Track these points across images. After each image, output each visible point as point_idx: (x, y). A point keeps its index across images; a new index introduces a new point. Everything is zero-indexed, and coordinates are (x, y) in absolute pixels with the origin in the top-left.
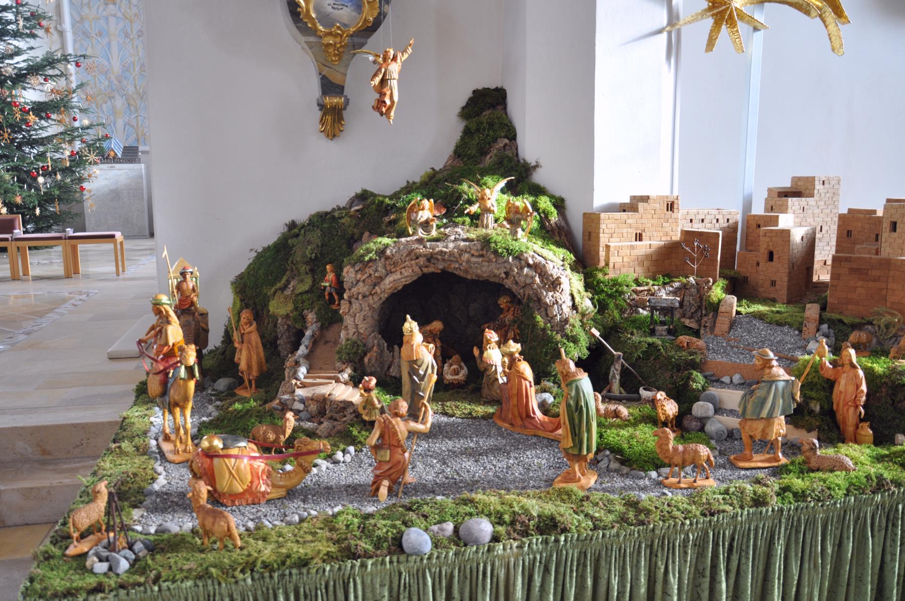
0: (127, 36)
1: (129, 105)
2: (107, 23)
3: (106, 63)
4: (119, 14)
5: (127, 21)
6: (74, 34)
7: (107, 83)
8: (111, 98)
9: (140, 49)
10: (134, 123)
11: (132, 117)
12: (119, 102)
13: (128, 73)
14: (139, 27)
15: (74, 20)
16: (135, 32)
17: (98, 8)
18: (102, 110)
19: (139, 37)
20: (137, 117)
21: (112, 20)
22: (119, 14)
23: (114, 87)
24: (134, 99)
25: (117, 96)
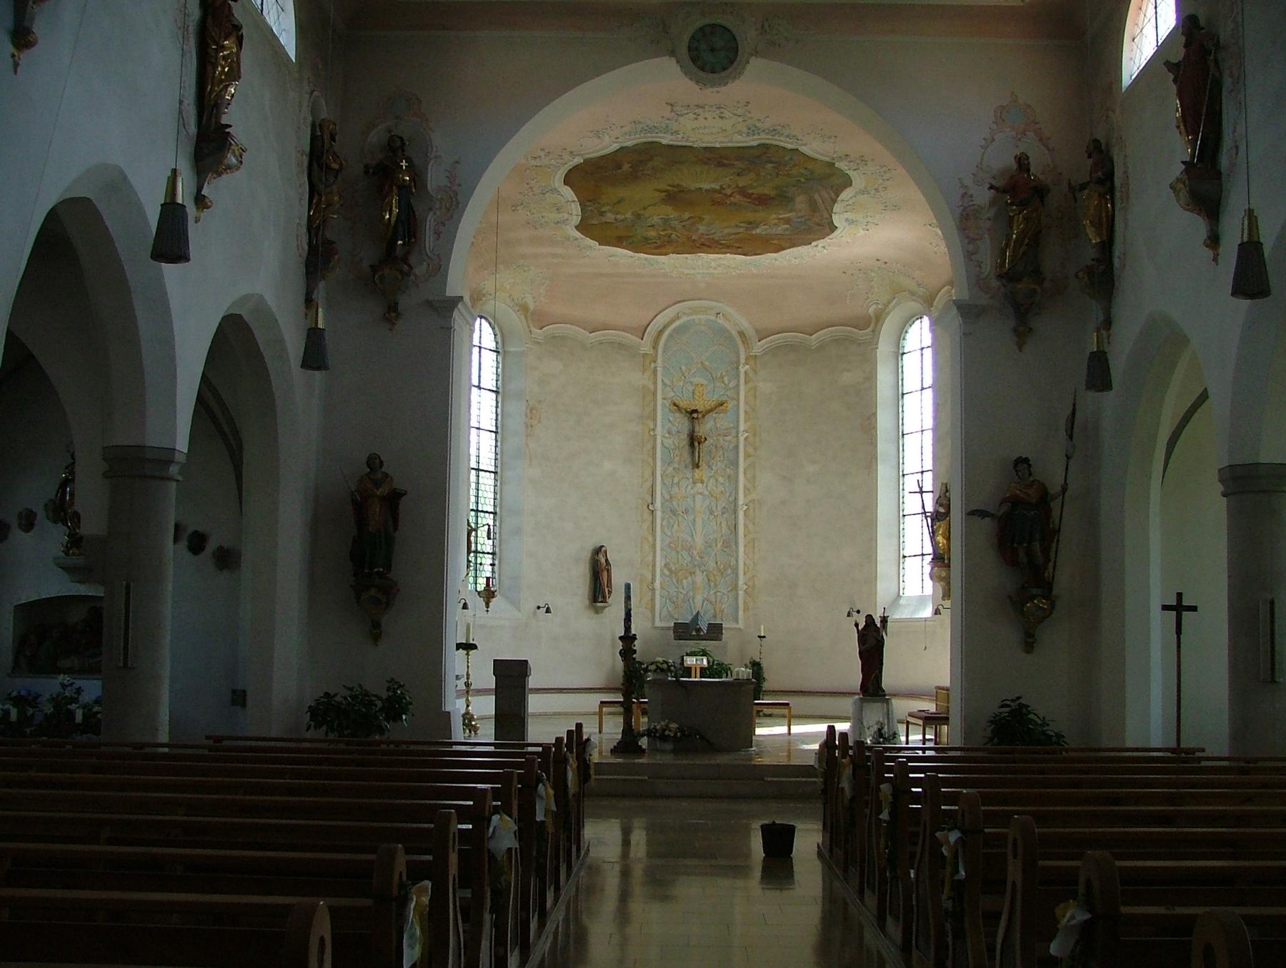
2: (694, 501)
3: (690, 539)
5: (713, 499)
6: (663, 512)
8: (693, 573)
9: (724, 525)
11: (712, 592)
12: (700, 578)
14: (724, 505)
18: (682, 583)
19: (723, 513)
20: (716, 592)
21: (699, 498)
23: (696, 563)
25: (698, 572)
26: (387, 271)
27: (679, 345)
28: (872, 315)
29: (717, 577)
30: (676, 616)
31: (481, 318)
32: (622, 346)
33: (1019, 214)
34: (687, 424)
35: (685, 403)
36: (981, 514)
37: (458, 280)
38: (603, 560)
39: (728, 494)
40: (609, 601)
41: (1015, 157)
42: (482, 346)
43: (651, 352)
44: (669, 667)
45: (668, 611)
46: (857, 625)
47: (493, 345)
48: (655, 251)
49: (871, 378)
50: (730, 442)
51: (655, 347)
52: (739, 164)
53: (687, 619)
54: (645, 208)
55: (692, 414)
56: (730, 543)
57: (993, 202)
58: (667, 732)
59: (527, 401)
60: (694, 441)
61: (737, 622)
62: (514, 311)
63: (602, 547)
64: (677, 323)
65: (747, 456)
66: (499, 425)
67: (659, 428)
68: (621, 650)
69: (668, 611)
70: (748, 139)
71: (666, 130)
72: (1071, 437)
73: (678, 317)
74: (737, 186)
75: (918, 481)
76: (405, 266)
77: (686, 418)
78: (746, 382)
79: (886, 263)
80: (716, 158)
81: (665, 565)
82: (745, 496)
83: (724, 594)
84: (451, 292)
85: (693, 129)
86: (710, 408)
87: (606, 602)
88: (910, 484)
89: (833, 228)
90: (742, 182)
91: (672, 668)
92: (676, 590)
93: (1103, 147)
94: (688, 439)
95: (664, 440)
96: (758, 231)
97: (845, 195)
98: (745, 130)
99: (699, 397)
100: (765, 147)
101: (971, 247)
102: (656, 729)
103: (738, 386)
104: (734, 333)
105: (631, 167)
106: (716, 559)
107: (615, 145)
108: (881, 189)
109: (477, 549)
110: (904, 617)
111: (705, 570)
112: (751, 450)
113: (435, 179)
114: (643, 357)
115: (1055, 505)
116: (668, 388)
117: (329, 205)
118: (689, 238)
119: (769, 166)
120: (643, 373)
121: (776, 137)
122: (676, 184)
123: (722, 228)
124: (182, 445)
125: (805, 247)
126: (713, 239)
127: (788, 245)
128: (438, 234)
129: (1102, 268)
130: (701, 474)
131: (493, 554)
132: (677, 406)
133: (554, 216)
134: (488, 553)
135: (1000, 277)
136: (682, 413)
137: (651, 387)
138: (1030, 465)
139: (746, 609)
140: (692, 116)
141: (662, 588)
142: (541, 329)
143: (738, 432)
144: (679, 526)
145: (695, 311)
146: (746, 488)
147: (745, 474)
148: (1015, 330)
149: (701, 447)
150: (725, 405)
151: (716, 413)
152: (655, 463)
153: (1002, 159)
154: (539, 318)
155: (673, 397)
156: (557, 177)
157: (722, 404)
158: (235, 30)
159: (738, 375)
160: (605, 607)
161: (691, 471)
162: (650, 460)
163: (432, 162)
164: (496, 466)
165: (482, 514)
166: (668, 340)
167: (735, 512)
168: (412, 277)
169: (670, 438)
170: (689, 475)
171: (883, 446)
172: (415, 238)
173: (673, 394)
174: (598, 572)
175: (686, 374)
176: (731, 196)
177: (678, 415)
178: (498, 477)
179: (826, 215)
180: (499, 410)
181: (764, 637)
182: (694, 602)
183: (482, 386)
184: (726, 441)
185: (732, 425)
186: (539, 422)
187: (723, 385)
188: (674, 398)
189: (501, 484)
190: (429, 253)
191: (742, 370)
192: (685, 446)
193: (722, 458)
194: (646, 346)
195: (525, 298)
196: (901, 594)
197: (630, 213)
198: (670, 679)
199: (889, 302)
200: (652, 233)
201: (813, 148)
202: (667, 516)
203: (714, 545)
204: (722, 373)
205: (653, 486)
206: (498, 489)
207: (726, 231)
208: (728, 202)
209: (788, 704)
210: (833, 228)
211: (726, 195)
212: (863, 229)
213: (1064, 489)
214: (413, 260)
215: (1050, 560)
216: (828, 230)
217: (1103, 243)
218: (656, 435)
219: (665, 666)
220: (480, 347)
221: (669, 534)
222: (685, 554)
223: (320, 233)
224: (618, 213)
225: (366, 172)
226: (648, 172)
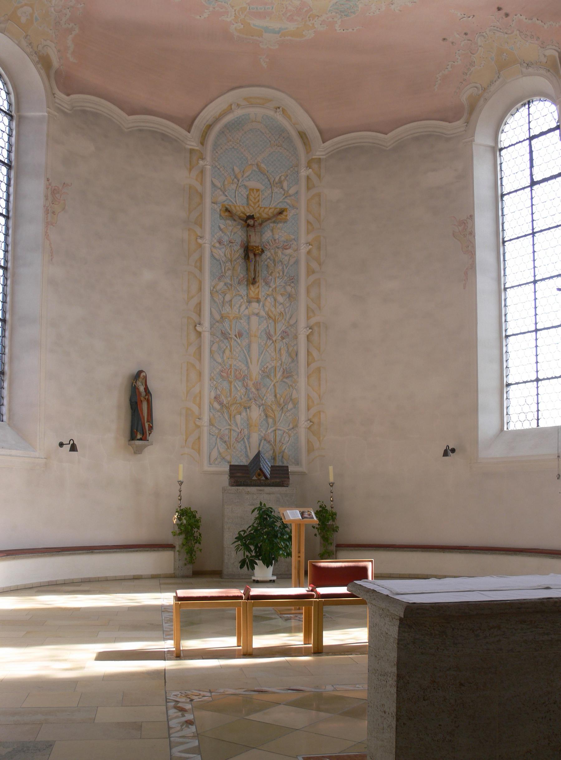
0: (269, 337)
1: (267, 416)
2: (249, 323)
4: (263, 313)
5: (271, 321)
6: (212, 334)
7: (243, 390)
9: (284, 352)
10: (271, 437)
11: (269, 431)
12: (256, 413)
13: (268, 380)
14: (284, 328)
15: (214, 319)
16: (278, 333)
19: (283, 338)
20: (275, 430)
21: (254, 319)
22: (263, 313)
23: (251, 396)
24: (272, 410)
25: (254, 407)
27: (231, 143)
30: (228, 458)
32: (164, 137)
34: (240, 234)
38: (142, 389)
39: (288, 316)
40: (150, 438)
45: (219, 452)
62: (32, 61)
65: (310, 272)
69: (219, 452)
73: (229, 110)
77: (239, 227)
78: (308, 188)
92: (229, 427)
94: (243, 250)
95: (214, 250)
99: (255, 204)
106: (275, 391)
111: (262, 405)
112: (314, 265)
116: (219, 190)
120: (190, 170)
130: (257, 292)
132: (229, 211)
136: (235, 220)
141: (211, 424)
142: (68, 95)
144: (231, 351)
147: (308, 291)
150: (285, 213)
151: (274, 222)
155: (224, 201)
157: (281, 213)
160: (145, 446)
161: (245, 288)
170: (243, 290)
173: (223, 198)
174: (136, 403)
175: (240, 176)
177: (229, 222)
180: (11, 189)
182: (249, 443)
186: (64, 209)
188: (225, 203)
189: (13, 282)
192: (238, 258)
193: (281, 273)
199: (492, 83)
202: (218, 340)
203: (272, 374)
204: (280, 177)
221: (220, 360)
222: (238, 384)
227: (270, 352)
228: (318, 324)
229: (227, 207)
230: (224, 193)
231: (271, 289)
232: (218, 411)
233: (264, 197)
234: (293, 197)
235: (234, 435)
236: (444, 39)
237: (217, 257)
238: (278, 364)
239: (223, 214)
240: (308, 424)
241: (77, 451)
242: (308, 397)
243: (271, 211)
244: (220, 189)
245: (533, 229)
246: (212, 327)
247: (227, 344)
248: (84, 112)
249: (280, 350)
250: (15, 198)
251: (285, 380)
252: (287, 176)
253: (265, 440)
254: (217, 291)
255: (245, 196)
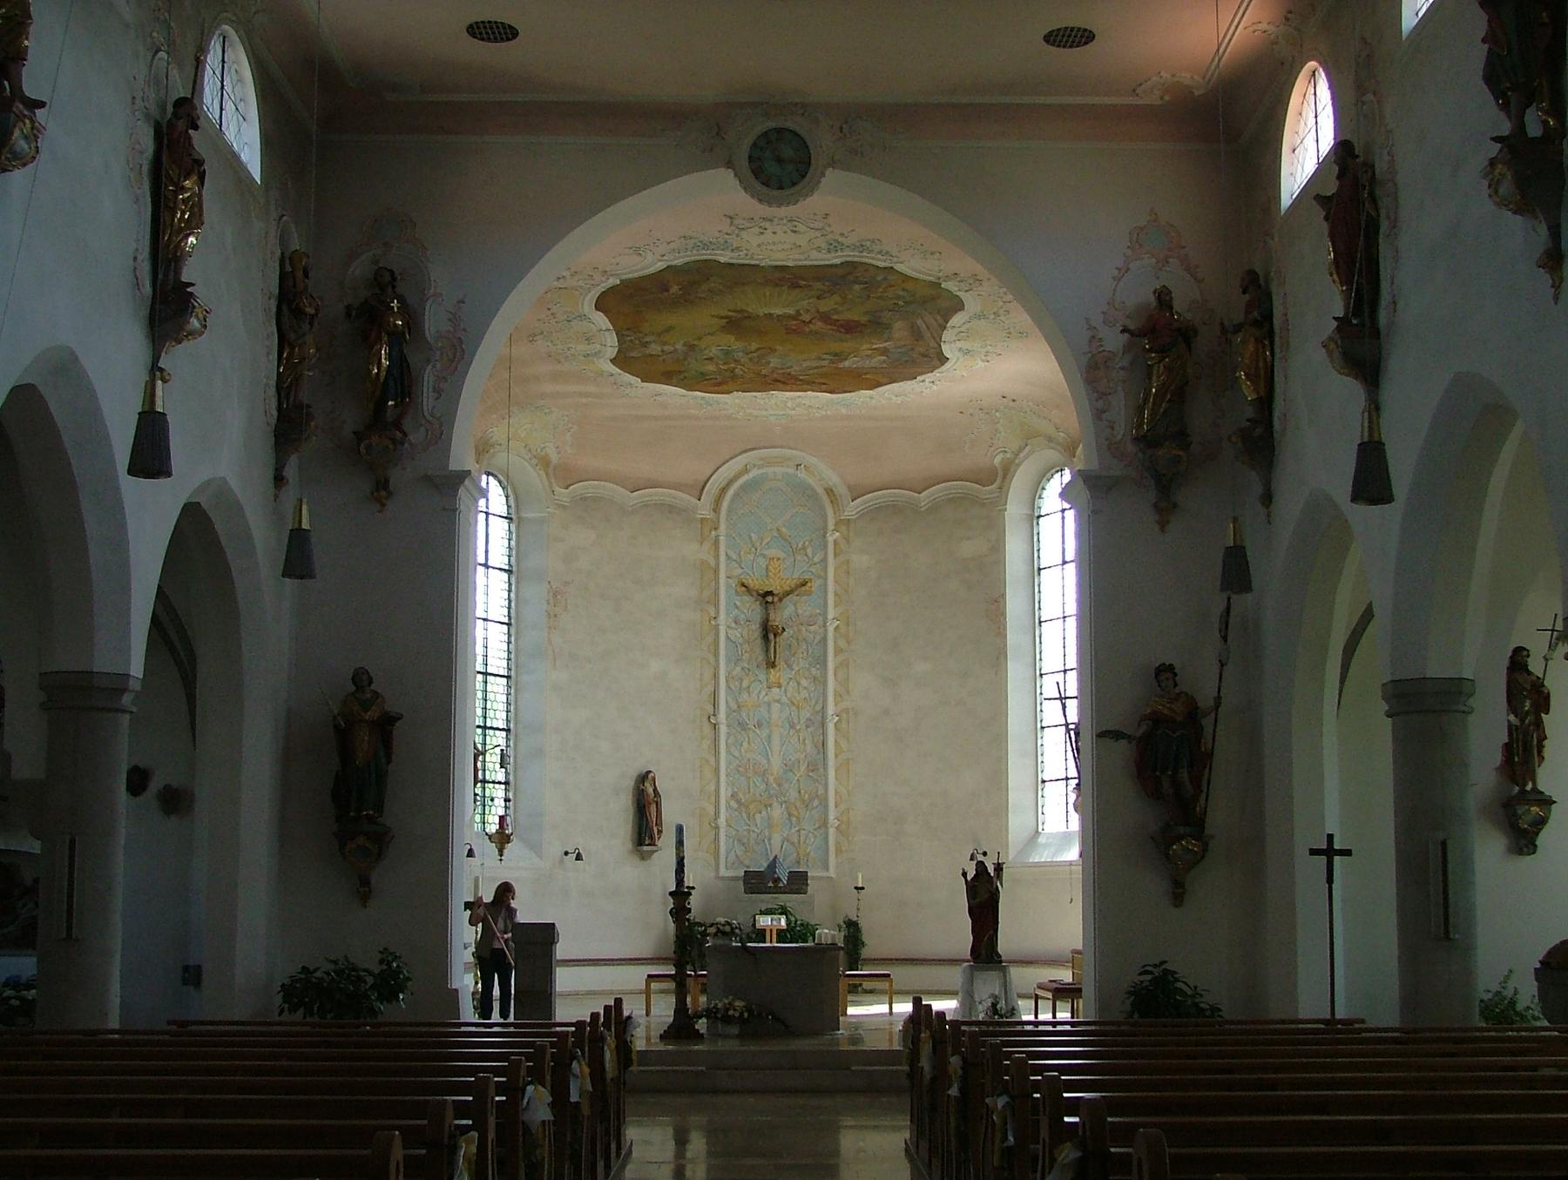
0: (792, 726)
1: (790, 815)
4: (784, 699)
5: (794, 708)
7: (763, 787)
11: (794, 830)
12: (777, 812)
13: (791, 774)
14: (808, 715)
15: (730, 708)
17: (760, 692)
19: (807, 727)
20: (799, 831)
21: (776, 706)
22: (784, 699)
23: (772, 792)
24: (796, 807)
26: (375, 439)
28: (997, 465)
29: (800, 811)
30: (747, 862)
31: (488, 475)
32: (670, 509)
33: (1159, 362)
35: (757, 583)
36: (1115, 735)
37: (461, 456)
38: (650, 790)
39: (813, 702)
40: (659, 843)
41: (1155, 292)
42: (490, 512)
43: (710, 515)
44: (732, 929)
45: (737, 856)
46: (964, 874)
47: (503, 511)
48: (712, 389)
49: (997, 549)
50: (815, 633)
51: (716, 509)
52: (818, 285)
53: (762, 866)
54: (700, 339)
55: (766, 598)
56: (817, 767)
57: (1127, 348)
58: (731, 1012)
59: (549, 582)
60: (768, 632)
61: (828, 870)
63: (650, 772)
64: (745, 478)
65: (838, 651)
66: (513, 615)
67: (722, 616)
68: (672, 909)
69: (737, 856)
70: (829, 256)
71: (725, 246)
72: (1225, 639)
73: (746, 470)
74: (818, 312)
75: (1058, 683)
76: (398, 433)
77: (758, 603)
78: (836, 555)
79: (1014, 400)
80: (788, 278)
81: (732, 796)
82: (836, 705)
83: (809, 832)
84: (454, 466)
85: (759, 246)
86: (789, 589)
87: (654, 845)
88: (1049, 687)
89: (943, 360)
90: (826, 306)
91: (737, 931)
93: (1262, 282)
95: (730, 631)
96: (847, 364)
97: (957, 320)
98: (824, 245)
100: (852, 266)
101: (1100, 404)
102: (718, 1009)
103: (824, 560)
104: (820, 491)
105: (680, 289)
107: (660, 263)
108: (1001, 312)
109: (485, 778)
110: (1043, 860)
111: (785, 802)
112: (842, 643)
113: (434, 322)
114: (702, 523)
115: (1207, 723)
116: (734, 563)
117: (302, 360)
118: (759, 374)
119: (857, 287)
121: (865, 254)
122: (738, 309)
123: (800, 360)
124: (137, 669)
125: (909, 382)
126: (789, 374)
127: (885, 380)
128: (438, 391)
129: (1259, 431)
130: (778, 675)
131: (506, 783)
132: (745, 587)
133: (583, 347)
134: (500, 783)
135: (1136, 440)
136: (752, 595)
137: (712, 562)
138: (1175, 675)
139: (839, 851)
140: (757, 230)
142: (567, 488)
143: (825, 623)
144: (749, 743)
145: (768, 462)
146: (838, 695)
148: (1155, 506)
149: (778, 640)
150: (809, 584)
151: (797, 595)
152: (717, 661)
153: (1138, 293)
154: (565, 475)
156: (586, 303)
157: (804, 584)
158: (196, 167)
159: (825, 547)
162: (712, 659)
163: (429, 302)
164: (509, 669)
165: (491, 732)
166: (732, 500)
167: (823, 725)
168: (406, 445)
169: (736, 629)
170: (762, 677)
171: (1015, 637)
172: (410, 395)
173: (741, 571)
175: (758, 544)
176: (810, 321)
177: (747, 598)
178: (512, 683)
179: (933, 344)
180: (512, 595)
181: (863, 888)
182: (770, 844)
183: (490, 564)
184: (810, 633)
185: (818, 611)
187: (805, 557)
189: (516, 690)
190: (426, 414)
191: (830, 539)
192: (756, 639)
193: (805, 654)
194: (704, 509)
195: (544, 447)
196: (1040, 830)
197: (682, 342)
198: (734, 944)
199: (1021, 449)
200: (711, 367)
201: (910, 265)
205: (715, 694)
206: (512, 698)
207: (809, 363)
208: (807, 329)
209: (889, 975)
210: (943, 360)
211: (804, 322)
212: (983, 361)
213: (1218, 701)
214: (407, 424)
215: (1202, 791)
216: (936, 362)
217: (1260, 399)
218: (718, 625)
219: (727, 928)
220: (487, 514)
221: (737, 754)
223: (293, 393)
224: (665, 344)
225: (348, 315)
226: (703, 296)
227: (793, 742)
228: (847, 711)
229: (744, 581)
230: (740, 565)
231: (793, 672)
232: (736, 810)
233: (785, 566)
234: (818, 565)
235: (753, 835)
236: (961, 412)
237: (733, 638)
238: (803, 756)
239: (739, 589)
240: (837, 823)
241: (582, 860)
242: (836, 792)
243: (794, 581)
244: (735, 560)
245: (1064, 612)
246: (727, 717)
247: (745, 736)
248: (586, 499)
249: (804, 740)
250: (516, 606)
251: (811, 774)
252: (812, 540)
253: (788, 841)
254: (733, 678)
255: (764, 566)
